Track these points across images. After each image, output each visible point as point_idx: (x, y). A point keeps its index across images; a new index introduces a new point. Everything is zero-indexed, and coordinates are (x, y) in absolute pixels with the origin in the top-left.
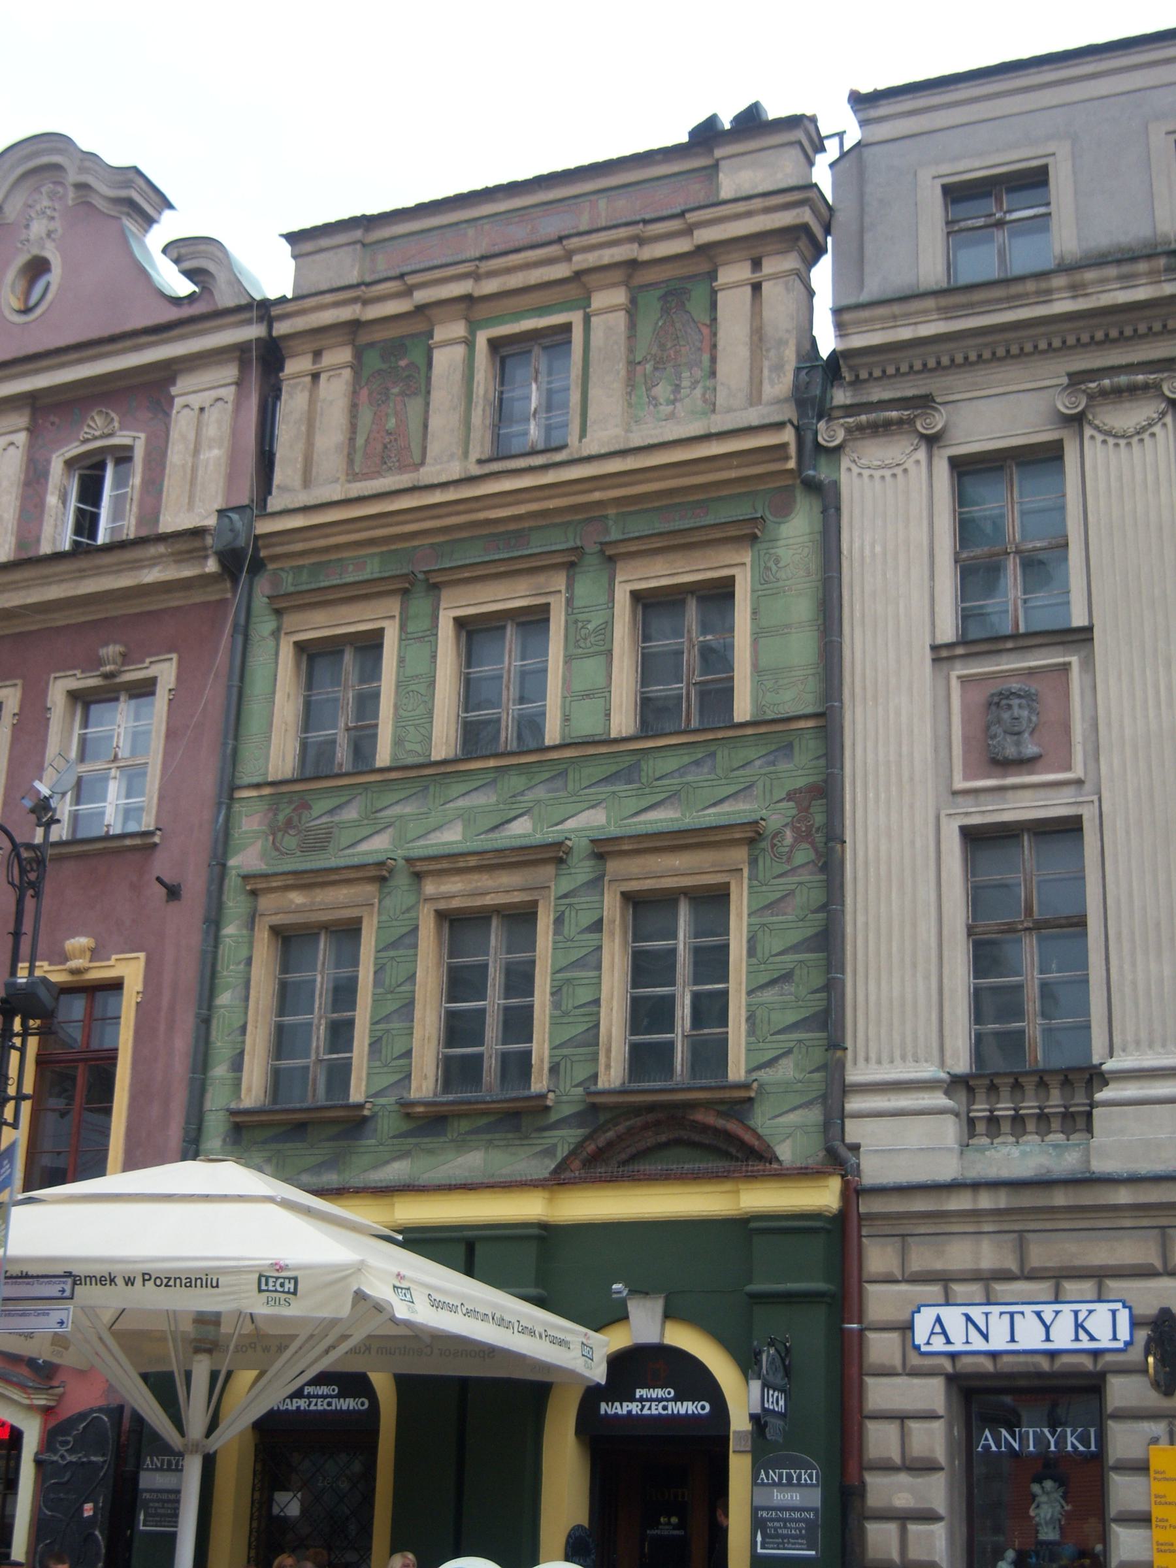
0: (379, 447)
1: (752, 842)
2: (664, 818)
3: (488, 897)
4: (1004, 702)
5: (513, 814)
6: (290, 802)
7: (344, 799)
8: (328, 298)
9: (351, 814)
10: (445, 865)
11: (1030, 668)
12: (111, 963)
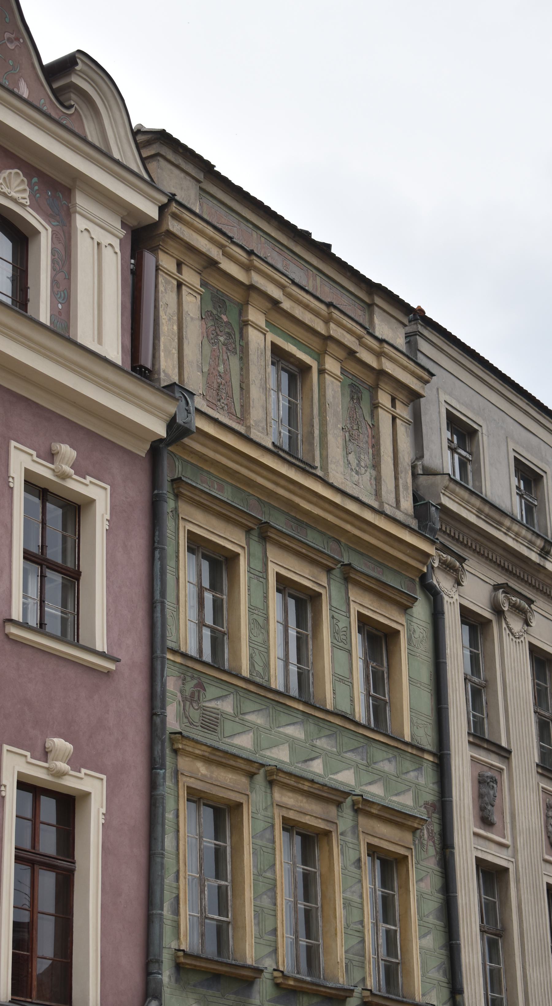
0: (215, 386)
1: (414, 831)
3: (308, 817)
4: (491, 784)
5: (313, 756)
6: (193, 678)
7: (225, 693)
8: (210, 231)
10: (292, 782)
11: (492, 765)
12: (82, 775)
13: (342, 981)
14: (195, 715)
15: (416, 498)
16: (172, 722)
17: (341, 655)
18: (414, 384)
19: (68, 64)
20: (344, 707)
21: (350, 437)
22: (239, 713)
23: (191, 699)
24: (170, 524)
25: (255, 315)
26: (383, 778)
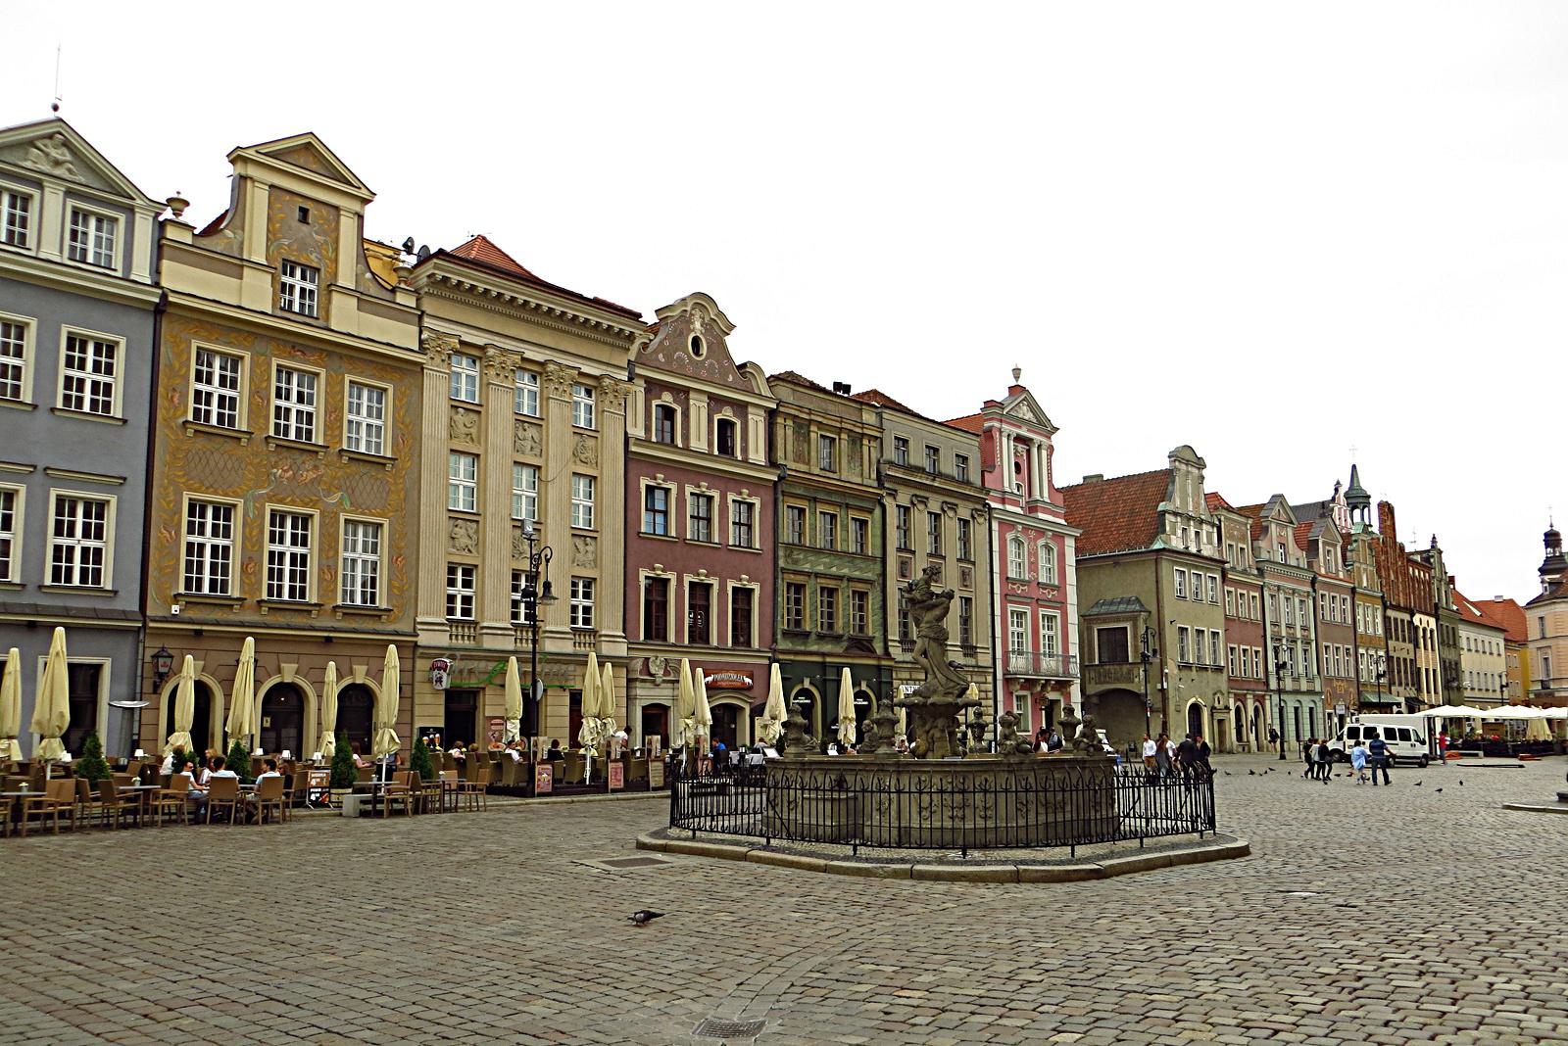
2: (857, 574)
9: (801, 556)
13: (841, 632)
14: (789, 560)
15: (878, 472)
16: (781, 563)
17: (844, 533)
18: (878, 435)
19: (744, 366)
20: (845, 549)
21: (851, 458)
22: (805, 557)
23: (787, 557)
24: (780, 505)
25: (813, 428)
26: (860, 569)
